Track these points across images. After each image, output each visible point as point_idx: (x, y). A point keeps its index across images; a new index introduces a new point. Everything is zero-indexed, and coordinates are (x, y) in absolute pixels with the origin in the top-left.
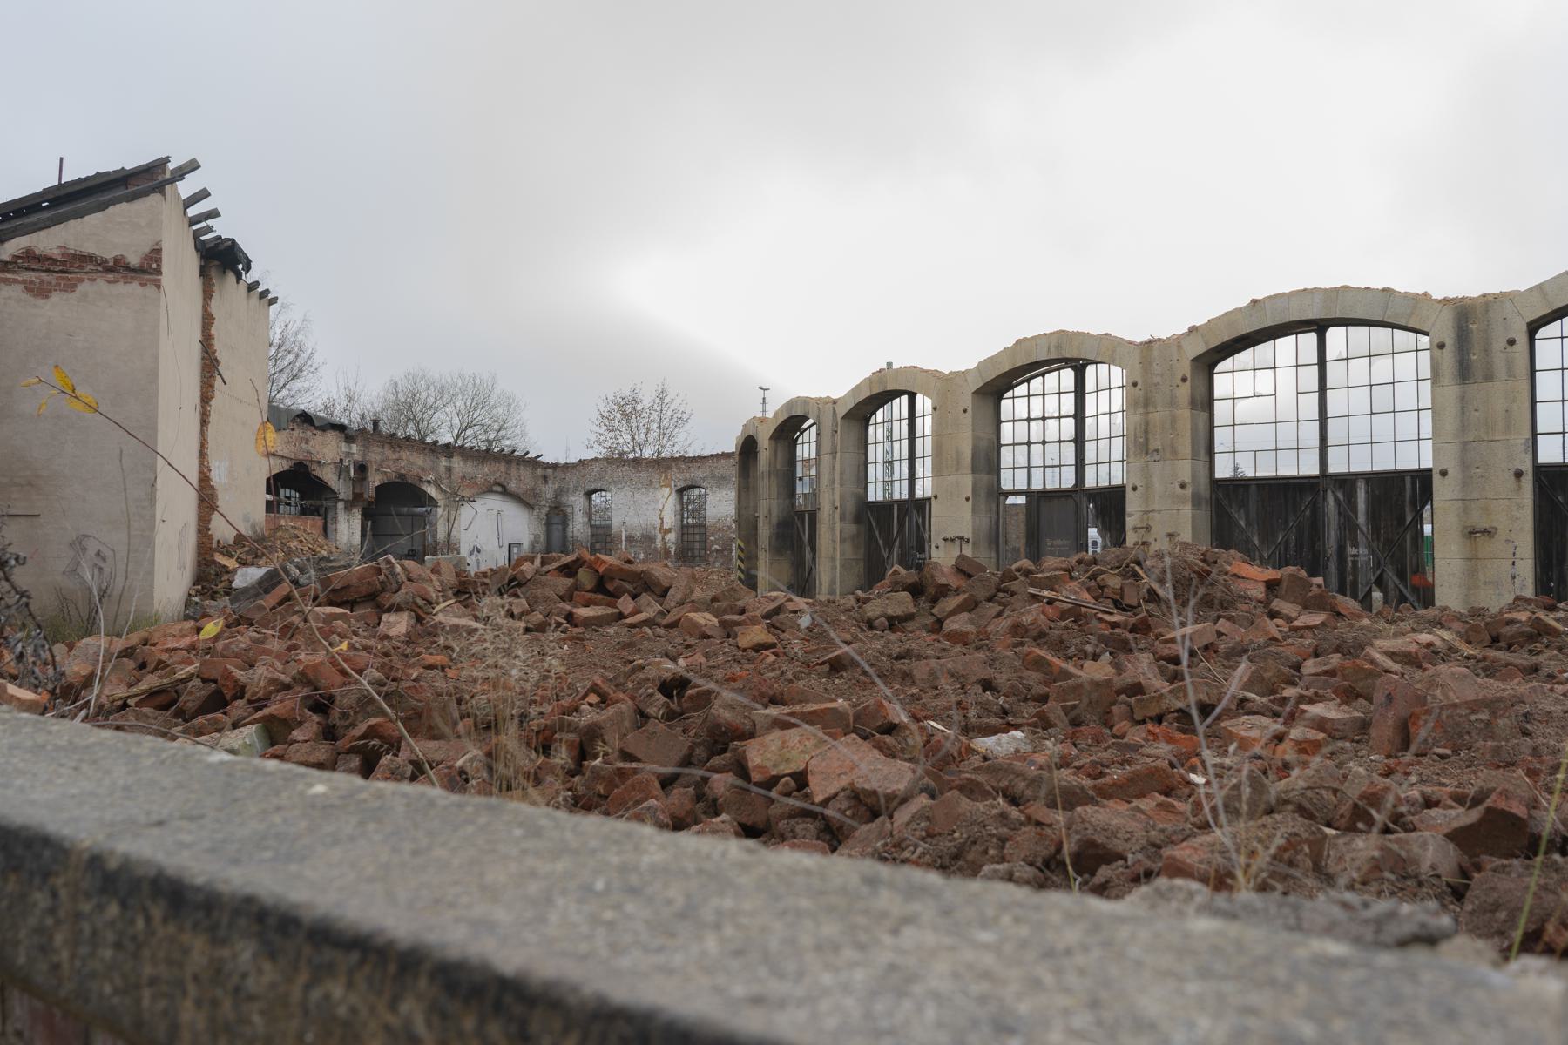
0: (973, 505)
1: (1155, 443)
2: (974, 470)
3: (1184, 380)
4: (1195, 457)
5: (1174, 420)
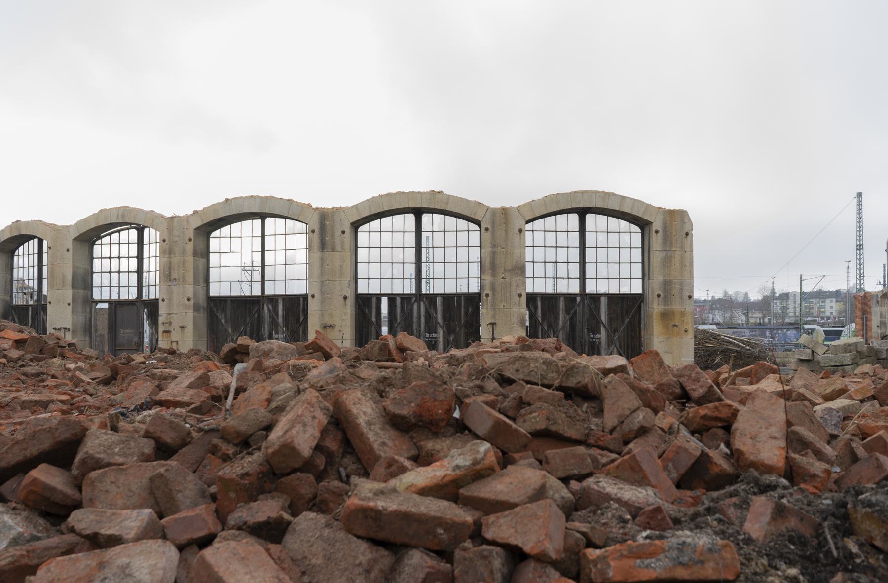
0: (73, 309)
1: (174, 275)
2: (73, 287)
3: (190, 240)
4: (196, 283)
5: (184, 262)
